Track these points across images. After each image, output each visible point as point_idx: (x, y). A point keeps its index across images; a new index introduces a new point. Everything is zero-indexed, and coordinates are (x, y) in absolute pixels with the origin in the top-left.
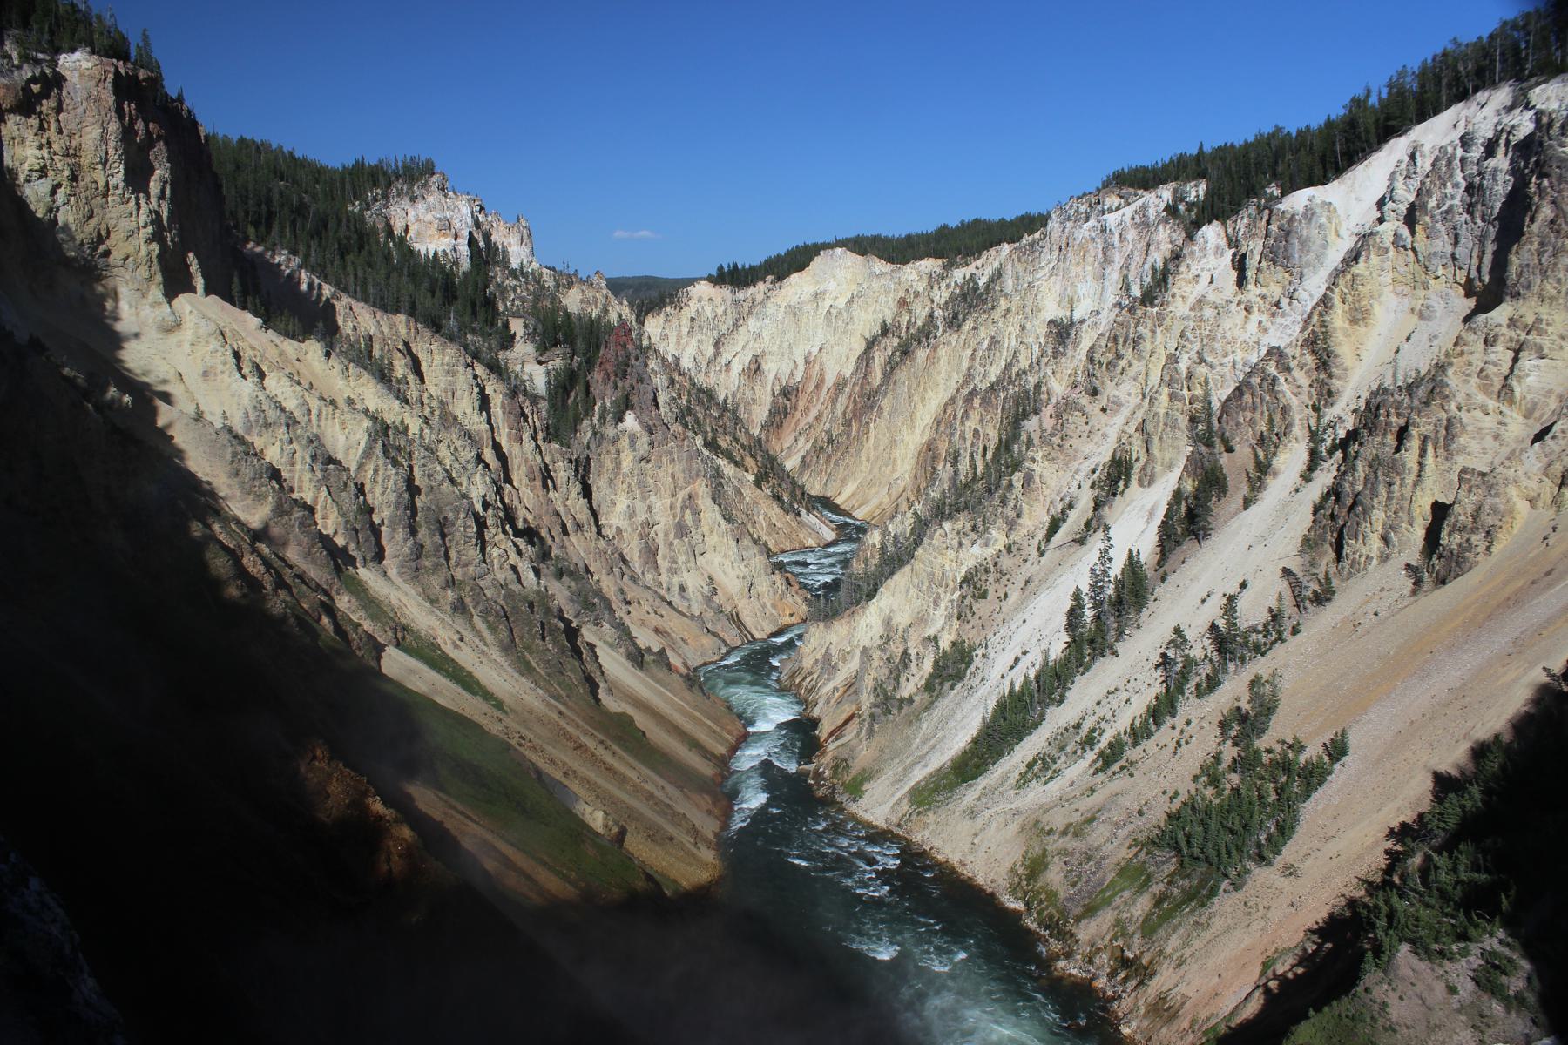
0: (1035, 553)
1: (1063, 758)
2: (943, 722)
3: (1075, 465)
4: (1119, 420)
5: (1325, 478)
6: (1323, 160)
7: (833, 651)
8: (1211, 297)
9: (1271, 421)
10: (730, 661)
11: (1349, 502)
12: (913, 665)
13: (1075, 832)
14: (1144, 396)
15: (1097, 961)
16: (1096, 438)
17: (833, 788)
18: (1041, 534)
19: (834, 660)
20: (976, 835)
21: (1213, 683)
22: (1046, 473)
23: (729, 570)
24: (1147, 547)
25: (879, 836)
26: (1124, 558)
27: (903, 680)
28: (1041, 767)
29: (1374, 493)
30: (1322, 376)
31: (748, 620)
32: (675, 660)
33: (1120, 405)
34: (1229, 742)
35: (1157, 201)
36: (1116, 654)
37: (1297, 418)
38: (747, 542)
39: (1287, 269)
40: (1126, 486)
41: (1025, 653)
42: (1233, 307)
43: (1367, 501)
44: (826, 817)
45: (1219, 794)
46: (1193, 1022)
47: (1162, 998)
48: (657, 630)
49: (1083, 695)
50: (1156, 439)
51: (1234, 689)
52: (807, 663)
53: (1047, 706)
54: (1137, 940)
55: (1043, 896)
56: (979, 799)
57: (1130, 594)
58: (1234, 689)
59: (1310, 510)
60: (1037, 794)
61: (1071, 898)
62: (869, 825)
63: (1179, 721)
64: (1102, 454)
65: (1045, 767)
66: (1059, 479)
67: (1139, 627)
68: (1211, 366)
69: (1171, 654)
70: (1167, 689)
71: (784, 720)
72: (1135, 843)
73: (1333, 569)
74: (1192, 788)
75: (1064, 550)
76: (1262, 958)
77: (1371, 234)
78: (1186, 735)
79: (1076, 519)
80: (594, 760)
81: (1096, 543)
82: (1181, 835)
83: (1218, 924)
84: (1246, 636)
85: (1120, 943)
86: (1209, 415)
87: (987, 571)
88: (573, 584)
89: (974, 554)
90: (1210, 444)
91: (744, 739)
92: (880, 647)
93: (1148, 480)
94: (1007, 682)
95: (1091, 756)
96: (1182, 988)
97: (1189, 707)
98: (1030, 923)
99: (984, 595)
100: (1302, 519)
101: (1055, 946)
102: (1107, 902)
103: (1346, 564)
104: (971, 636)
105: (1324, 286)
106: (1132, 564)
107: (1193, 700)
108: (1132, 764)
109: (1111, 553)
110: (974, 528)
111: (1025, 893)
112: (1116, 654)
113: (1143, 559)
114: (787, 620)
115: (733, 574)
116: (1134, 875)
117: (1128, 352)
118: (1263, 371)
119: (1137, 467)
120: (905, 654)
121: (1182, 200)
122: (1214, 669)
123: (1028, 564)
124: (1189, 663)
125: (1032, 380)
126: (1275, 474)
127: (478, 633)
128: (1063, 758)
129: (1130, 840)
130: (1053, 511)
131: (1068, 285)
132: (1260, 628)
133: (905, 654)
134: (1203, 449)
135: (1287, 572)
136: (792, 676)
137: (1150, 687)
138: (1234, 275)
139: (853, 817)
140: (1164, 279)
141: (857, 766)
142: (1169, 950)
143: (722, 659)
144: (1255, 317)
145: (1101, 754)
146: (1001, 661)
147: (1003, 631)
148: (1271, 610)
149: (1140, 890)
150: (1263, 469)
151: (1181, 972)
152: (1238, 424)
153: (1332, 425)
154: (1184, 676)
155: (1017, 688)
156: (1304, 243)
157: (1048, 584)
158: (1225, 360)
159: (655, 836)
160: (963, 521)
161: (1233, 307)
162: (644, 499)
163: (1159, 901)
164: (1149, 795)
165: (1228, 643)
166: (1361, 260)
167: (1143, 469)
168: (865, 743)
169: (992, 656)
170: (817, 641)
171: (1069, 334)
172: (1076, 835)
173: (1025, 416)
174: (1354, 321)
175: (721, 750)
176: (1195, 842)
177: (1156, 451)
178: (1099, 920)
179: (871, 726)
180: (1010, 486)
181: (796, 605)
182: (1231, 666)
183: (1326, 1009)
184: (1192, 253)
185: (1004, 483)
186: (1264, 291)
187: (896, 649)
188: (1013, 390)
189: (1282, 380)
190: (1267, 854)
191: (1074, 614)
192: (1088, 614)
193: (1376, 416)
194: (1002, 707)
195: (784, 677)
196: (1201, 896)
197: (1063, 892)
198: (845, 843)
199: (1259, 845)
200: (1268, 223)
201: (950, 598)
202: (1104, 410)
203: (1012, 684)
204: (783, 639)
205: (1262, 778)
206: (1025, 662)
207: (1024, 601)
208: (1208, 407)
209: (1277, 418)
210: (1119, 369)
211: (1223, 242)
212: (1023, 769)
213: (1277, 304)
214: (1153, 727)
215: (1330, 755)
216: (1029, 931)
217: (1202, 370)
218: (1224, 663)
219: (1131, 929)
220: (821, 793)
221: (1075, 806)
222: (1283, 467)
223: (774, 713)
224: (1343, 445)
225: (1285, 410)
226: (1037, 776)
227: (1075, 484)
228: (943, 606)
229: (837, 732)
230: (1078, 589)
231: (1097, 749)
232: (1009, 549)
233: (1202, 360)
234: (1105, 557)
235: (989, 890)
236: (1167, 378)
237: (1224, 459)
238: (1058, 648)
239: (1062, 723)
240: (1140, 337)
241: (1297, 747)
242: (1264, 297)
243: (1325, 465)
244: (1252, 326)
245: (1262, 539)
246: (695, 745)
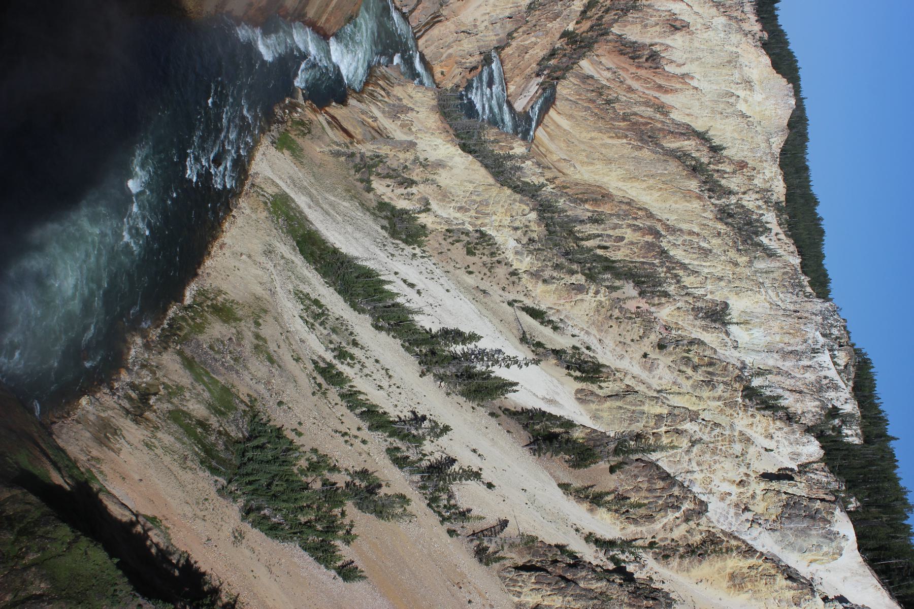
0: (511, 297)
1: (325, 332)
2: (351, 221)
3: (594, 331)
4: (636, 370)
5: (589, 554)
6: (880, 548)
7: (411, 115)
8: (752, 450)
9: (640, 506)
10: (395, 15)
11: (569, 576)
12: (401, 190)
13: (260, 347)
14: (659, 392)
15: (144, 372)
16: (619, 350)
17: (283, 122)
18: (529, 303)
19: (402, 116)
20: (249, 256)
21: (401, 462)
22: (585, 305)
23: (483, 10)
24: (521, 399)
25: (241, 168)
27: (388, 181)
28: (316, 313)
29: (577, 597)
30: (682, 550)
31: (436, 31)
33: (650, 370)
34: (349, 479)
35: (842, 399)
36: (423, 374)
37: (644, 529)
38: (510, 26)
39: (779, 517)
40: (576, 378)
41: (419, 292)
42: (743, 470)
43: (570, 591)
44: (255, 117)
45: (302, 472)
46: (98, 460)
47: (116, 431)
49: (383, 347)
50: (619, 403)
51: (397, 481)
52: (398, 91)
53: (372, 315)
54: (166, 406)
55: (198, 321)
56: (283, 257)
57: (478, 385)
58: (397, 481)
59: (561, 541)
60: (291, 310)
61: (199, 345)
62: (251, 157)
63: (365, 433)
64: (605, 356)
65: (316, 316)
66: (580, 317)
67: (448, 394)
68: (688, 451)
69: (426, 424)
70: (394, 422)
71: (344, 72)
72: (253, 400)
73: (508, 563)
74: (307, 448)
75: (515, 324)
76: (159, 516)
77: (813, 591)
78: (353, 441)
79: (544, 333)
81: (523, 353)
82: (263, 440)
83: (187, 476)
84: (445, 489)
85: (162, 392)
86: (643, 451)
87: (493, 254)
89: (507, 241)
90: (616, 452)
91: (323, 35)
92: (416, 159)
93: (582, 397)
94: (392, 278)
95: (329, 356)
96: (126, 448)
97: (378, 442)
98: (173, 311)
99: (470, 252)
100: (551, 535)
101: (154, 334)
102: (198, 378)
103: (513, 574)
104: (432, 243)
105: (764, 550)
106: (505, 386)
107: (384, 446)
108: (324, 393)
110: (531, 240)
111: (200, 304)
112: (423, 374)
113: (509, 395)
114: (437, 70)
115: (478, 15)
116: (224, 401)
117: (699, 376)
118: (685, 498)
119: (594, 387)
120: (412, 183)
121: (843, 422)
122: (413, 462)
123: (501, 292)
124: (418, 441)
125: (672, 289)
126: (591, 511)
128: (325, 332)
129: (255, 395)
130: (551, 312)
131: (763, 322)
132: (452, 502)
133: (412, 183)
134: (612, 446)
135: (504, 524)
136: (385, 78)
137: (394, 407)
138: (773, 470)
139: (257, 142)
140: (768, 407)
141: (304, 142)
142: (159, 435)
143: (396, 8)
144: (734, 490)
145: (331, 366)
146: (410, 272)
147: (438, 272)
148: (469, 511)
149: (210, 407)
150: (596, 500)
151: (140, 446)
152: (636, 476)
153: (637, 559)
154: (405, 437)
155: (386, 287)
156: (804, 532)
157: (484, 311)
158: (694, 464)
160: (537, 230)
161: (743, 470)
163: (202, 424)
164: (297, 410)
165: (438, 473)
166: (789, 583)
167: (592, 393)
168: (326, 149)
169: (415, 262)
170: (419, 99)
171: (715, 321)
172: (256, 347)
173: (638, 284)
174: (732, 576)
175: (311, 13)
176: (258, 452)
177: (608, 404)
178: (181, 372)
179: (343, 154)
180: (572, 272)
181: (452, 78)
182: (417, 477)
183: (120, 572)
184: (794, 432)
185: (575, 267)
186: (759, 498)
187: (416, 174)
188: (661, 271)
189: (677, 514)
190: (252, 516)
191: (457, 336)
192: (458, 349)
193: (646, 598)
194: (368, 274)
195: (383, 69)
196: (210, 460)
197: (204, 339)
198: (232, 136)
199: (259, 509)
200: (822, 500)
201: (465, 220)
202: (645, 355)
203: (390, 282)
204: (418, 66)
205: (319, 509)
206: (411, 293)
207: (467, 289)
209: (643, 511)
210: (683, 368)
211: (803, 460)
212: (313, 296)
213: (747, 509)
214: (358, 411)
215: (343, 566)
216: (165, 310)
217: (685, 443)
218: (419, 471)
219: (175, 400)
220: (278, 111)
221: (282, 345)
222: (598, 517)
223: (348, 62)
224: (620, 570)
225: (650, 518)
226: (307, 309)
227: (576, 332)
228: (458, 215)
229: (335, 122)
230: (480, 338)
231: (335, 362)
232: (514, 273)
233: (693, 443)
235: (200, 272)
236: (676, 412)
237: (603, 465)
238: (424, 322)
239: (357, 329)
240: (714, 387)
241: (349, 538)
242: (753, 497)
243: (601, 554)
244: (726, 487)
245: (532, 501)
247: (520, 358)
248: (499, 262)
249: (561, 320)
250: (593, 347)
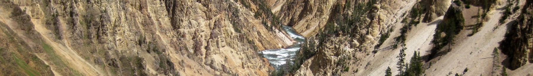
3: (395, 11)
22: (381, 14)
26: (412, 55)
81: (400, 48)
87: (349, 59)
88: (157, 55)
99: (347, 70)
106: (416, 58)
109: (406, 52)
123: (369, 55)
126: (487, 20)
162: (196, 20)
227: (395, 20)
230: (389, 68)
247: (401, 48)
248: (353, 56)
249: (388, 27)
250: (404, 12)
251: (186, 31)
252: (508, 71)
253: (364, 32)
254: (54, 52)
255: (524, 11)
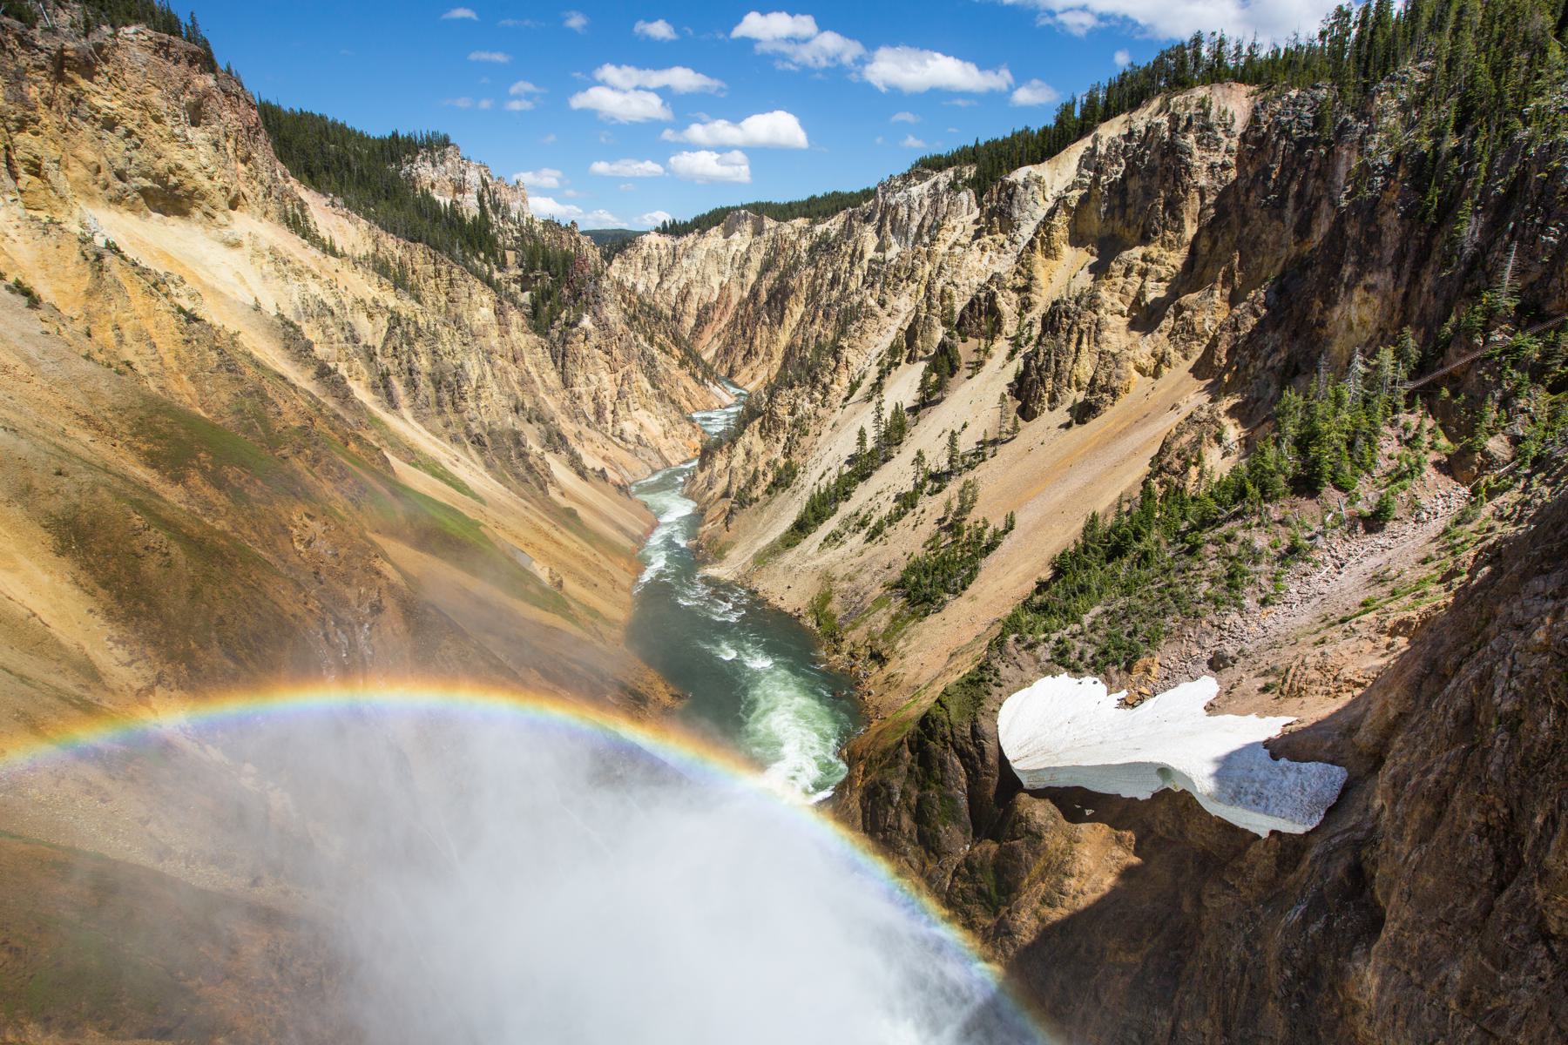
28: (835, 538)
32: (610, 474)
48: (604, 458)
49: (862, 495)
57: (894, 434)
58: (953, 487)
61: (844, 618)
63: (918, 510)
64: (885, 342)
80: (547, 535)
81: (876, 399)
95: (864, 532)
99: (806, 434)
104: (796, 458)
106: (897, 413)
120: (756, 470)
125: (857, 299)
126: (991, 357)
127: (470, 457)
133: (756, 470)
144: (988, 254)
147: (817, 455)
159: (584, 582)
187: (751, 468)
188: (844, 305)
208: (952, 312)
213: (1002, 246)
234: (879, 409)
244: (985, 260)
246: (621, 529)
251: (583, 390)
252: (1021, 423)
253: (827, 380)
254: (387, 428)
255: (1039, 343)
